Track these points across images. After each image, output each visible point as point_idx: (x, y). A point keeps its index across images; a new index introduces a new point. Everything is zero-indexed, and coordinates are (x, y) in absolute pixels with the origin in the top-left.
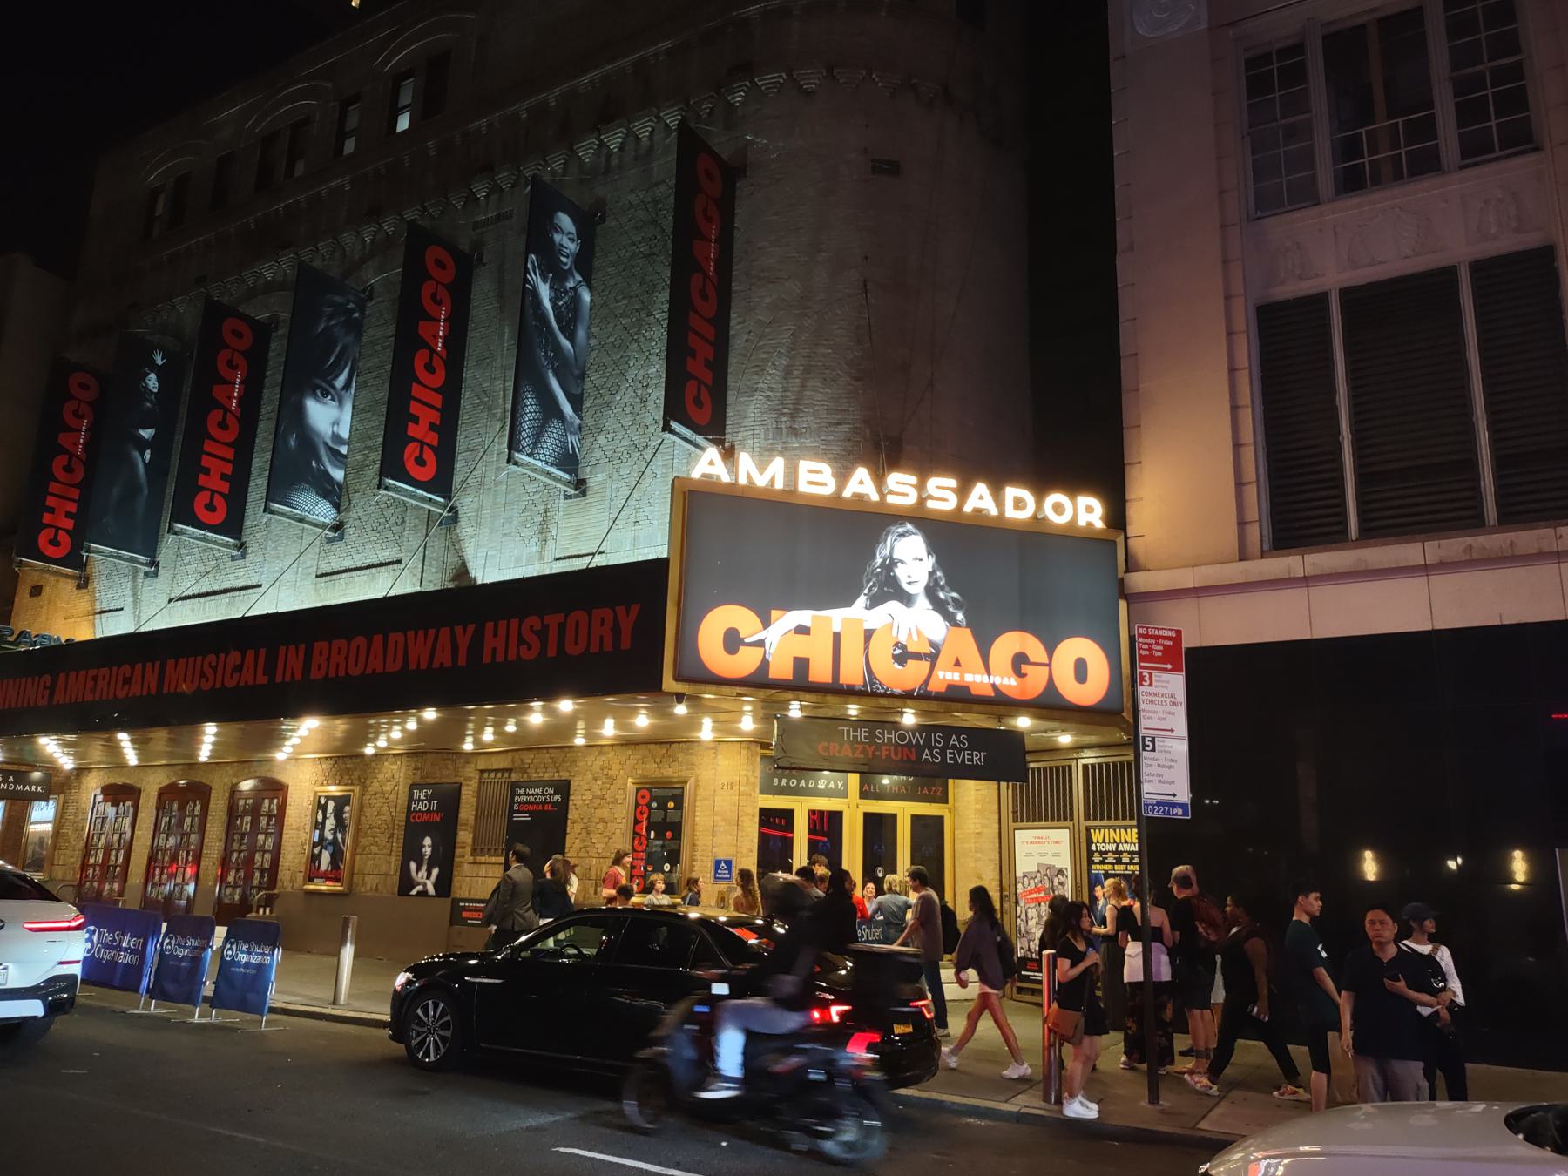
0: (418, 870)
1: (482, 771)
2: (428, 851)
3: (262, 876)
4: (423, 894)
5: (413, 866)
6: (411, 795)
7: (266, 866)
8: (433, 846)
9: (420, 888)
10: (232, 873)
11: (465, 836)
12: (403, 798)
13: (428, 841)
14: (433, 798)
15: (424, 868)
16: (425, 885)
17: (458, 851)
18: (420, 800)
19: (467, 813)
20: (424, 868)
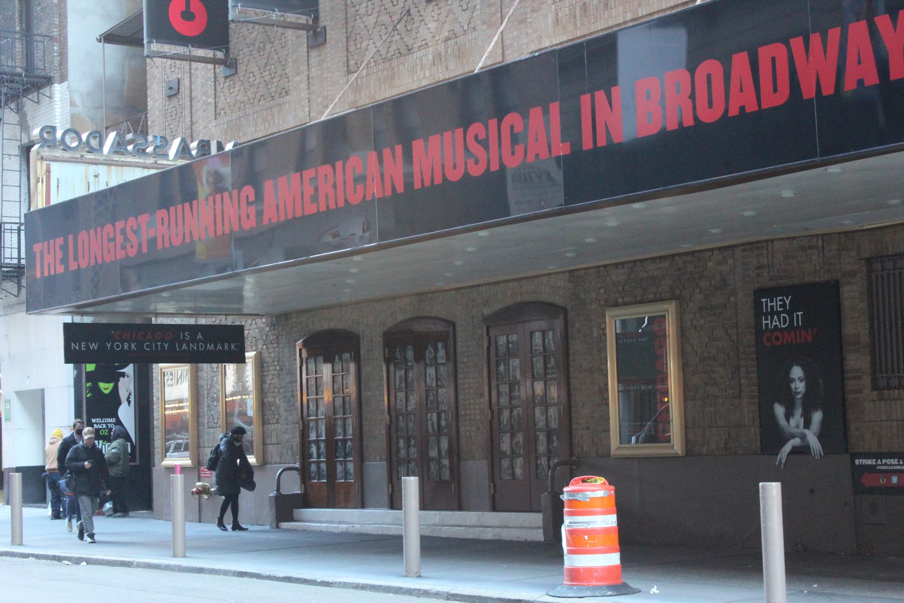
0: (788, 415)
1: (869, 261)
2: (800, 387)
3: (549, 441)
4: (802, 450)
5: (779, 410)
6: (757, 305)
7: (554, 425)
8: (808, 378)
9: (796, 441)
10: (506, 438)
11: (857, 361)
12: (746, 315)
13: (797, 372)
14: (794, 308)
15: (798, 412)
16: (803, 437)
17: (851, 384)
18: (773, 313)
19: (855, 324)
20: (798, 412)
